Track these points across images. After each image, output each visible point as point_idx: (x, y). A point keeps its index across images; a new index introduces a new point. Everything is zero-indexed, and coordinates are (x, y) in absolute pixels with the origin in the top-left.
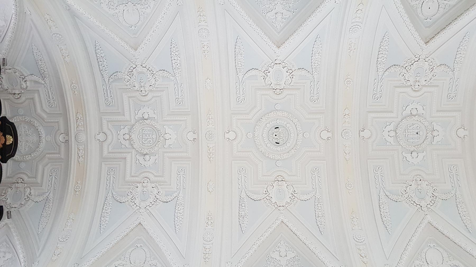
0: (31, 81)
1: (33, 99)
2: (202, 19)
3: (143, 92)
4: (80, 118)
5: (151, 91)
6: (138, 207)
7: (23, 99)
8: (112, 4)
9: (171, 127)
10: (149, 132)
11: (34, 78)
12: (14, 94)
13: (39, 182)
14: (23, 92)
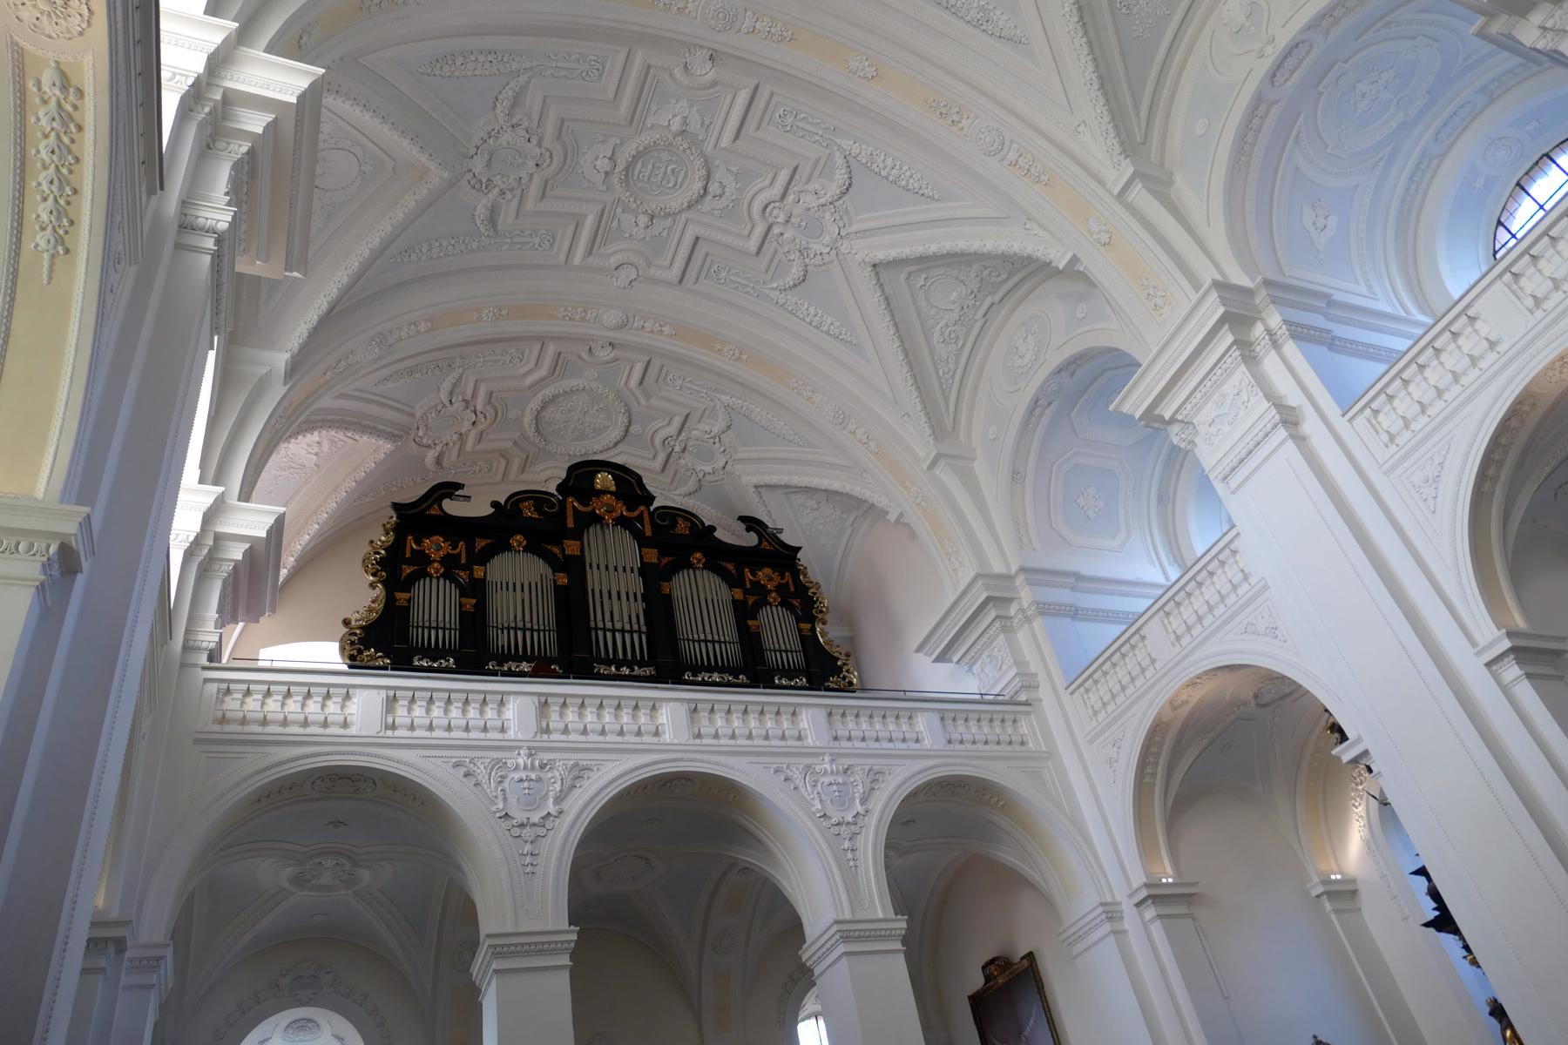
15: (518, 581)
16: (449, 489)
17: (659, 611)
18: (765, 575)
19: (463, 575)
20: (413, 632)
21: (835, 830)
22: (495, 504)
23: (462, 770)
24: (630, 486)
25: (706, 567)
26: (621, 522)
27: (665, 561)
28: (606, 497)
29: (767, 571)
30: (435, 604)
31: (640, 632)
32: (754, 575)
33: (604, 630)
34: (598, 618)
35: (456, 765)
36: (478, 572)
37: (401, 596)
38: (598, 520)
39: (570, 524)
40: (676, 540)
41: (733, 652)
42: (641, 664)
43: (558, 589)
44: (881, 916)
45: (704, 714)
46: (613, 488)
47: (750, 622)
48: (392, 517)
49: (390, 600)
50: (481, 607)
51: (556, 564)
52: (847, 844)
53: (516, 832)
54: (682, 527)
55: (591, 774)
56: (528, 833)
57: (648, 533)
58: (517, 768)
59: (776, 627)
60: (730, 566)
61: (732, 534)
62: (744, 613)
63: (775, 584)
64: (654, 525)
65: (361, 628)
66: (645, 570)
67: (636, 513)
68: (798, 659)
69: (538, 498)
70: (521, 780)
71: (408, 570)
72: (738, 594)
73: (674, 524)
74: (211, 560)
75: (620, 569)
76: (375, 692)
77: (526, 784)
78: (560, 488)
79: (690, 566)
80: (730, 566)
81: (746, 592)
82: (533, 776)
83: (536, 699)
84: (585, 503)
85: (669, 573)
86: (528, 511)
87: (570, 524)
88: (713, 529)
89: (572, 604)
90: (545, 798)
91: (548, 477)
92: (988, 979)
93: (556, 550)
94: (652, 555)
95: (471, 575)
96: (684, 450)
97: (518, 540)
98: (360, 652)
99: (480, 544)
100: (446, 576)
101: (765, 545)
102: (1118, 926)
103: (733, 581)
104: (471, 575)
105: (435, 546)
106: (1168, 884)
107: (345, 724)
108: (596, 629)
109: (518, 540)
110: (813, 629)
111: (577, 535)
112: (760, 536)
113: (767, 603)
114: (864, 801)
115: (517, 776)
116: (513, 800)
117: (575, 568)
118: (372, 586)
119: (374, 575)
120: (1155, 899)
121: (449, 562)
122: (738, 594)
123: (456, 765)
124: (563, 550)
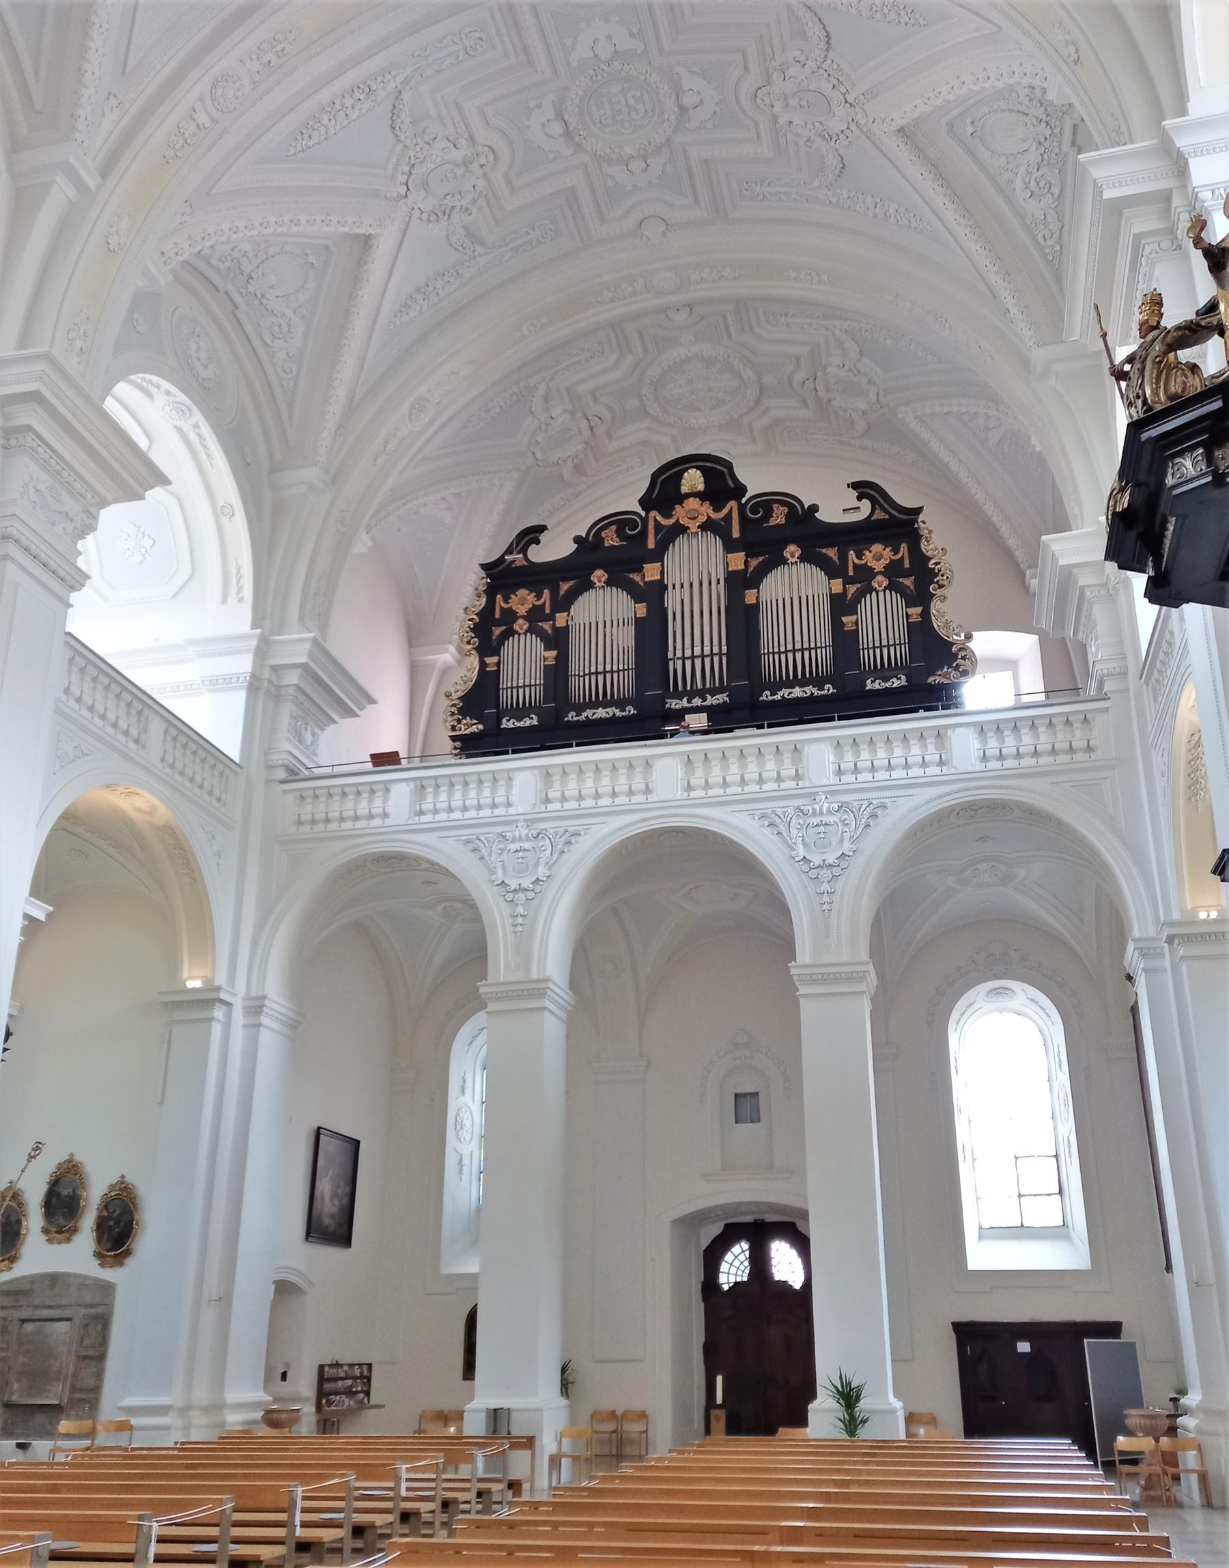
1: (593, 394)
2: (193, 127)
3: (483, 161)
4: (610, 295)
5: (472, 140)
6: (853, 126)
7: (598, 409)
8: (277, 329)
9: (569, 44)
10: (607, 106)
12: (592, 428)
13: (806, 349)
14: (580, 415)
16: (532, 535)
17: (743, 622)
18: (877, 556)
19: (547, 626)
21: (813, 874)
22: (577, 540)
23: (470, 847)
24: (721, 482)
25: (802, 559)
27: (754, 563)
28: (693, 503)
29: (877, 548)
30: (524, 661)
31: (720, 654)
32: (859, 556)
34: (677, 645)
35: (467, 842)
36: (561, 619)
37: (488, 660)
38: (680, 529)
39: (651, 544)
41: (824, 656)
42: (714, 692)
43: (639, 622)
44: (845, 959)
45: (698, 765)
46: (701, 487)
47: (844, 619)
49: (483, 665)
50: (563, 660)
51: (637, 593)
52: (825, 887)
53: (509, 897)
54: (779, 516)
55: (581, 839)
56: (521, 897)
57: (736, 534)
58: (514, 840)
60: (832, 553)
62: (840, 606)
63: (872, 564)
67: (725, 512)
68: (901, 652)
69: (621, 521)
70: (517, 851)
71: (497, 631)
73: (768, 514)
76: (404, 785)
77: (521, 854)
79: (784, 561)
80: (832, 553)
81: (848, 581)
82: (526, 845)
83: (536, 772)
84: (667, 515)
86: (611, 539)
87: (651, 544)
88: (814, 508)
89: (652, 633)
90: (537, 865)
91: (627, 497)
93: (636, 577)
94: (737, 561)
95: (554, 626)
96: (828, 390)
97: (599, 576)
98: (459, 721)
99: (565, 587)
100: (530, 630)
101: (879, 515)
103: (831, 570)
104: (554, 626)
105: (522, 601)
107: (385, 815)
109: (599, 576)
110: (926, 614)
111: (658, 555)
112: (874, 502)
113: (870, 590)
114: (854, 841)
115: (513, 847)
116: (510, 869)
117: (653, 595)
119: (469, 643)
121: (535, 615)
122: (837, 585)
124: (644, 576)
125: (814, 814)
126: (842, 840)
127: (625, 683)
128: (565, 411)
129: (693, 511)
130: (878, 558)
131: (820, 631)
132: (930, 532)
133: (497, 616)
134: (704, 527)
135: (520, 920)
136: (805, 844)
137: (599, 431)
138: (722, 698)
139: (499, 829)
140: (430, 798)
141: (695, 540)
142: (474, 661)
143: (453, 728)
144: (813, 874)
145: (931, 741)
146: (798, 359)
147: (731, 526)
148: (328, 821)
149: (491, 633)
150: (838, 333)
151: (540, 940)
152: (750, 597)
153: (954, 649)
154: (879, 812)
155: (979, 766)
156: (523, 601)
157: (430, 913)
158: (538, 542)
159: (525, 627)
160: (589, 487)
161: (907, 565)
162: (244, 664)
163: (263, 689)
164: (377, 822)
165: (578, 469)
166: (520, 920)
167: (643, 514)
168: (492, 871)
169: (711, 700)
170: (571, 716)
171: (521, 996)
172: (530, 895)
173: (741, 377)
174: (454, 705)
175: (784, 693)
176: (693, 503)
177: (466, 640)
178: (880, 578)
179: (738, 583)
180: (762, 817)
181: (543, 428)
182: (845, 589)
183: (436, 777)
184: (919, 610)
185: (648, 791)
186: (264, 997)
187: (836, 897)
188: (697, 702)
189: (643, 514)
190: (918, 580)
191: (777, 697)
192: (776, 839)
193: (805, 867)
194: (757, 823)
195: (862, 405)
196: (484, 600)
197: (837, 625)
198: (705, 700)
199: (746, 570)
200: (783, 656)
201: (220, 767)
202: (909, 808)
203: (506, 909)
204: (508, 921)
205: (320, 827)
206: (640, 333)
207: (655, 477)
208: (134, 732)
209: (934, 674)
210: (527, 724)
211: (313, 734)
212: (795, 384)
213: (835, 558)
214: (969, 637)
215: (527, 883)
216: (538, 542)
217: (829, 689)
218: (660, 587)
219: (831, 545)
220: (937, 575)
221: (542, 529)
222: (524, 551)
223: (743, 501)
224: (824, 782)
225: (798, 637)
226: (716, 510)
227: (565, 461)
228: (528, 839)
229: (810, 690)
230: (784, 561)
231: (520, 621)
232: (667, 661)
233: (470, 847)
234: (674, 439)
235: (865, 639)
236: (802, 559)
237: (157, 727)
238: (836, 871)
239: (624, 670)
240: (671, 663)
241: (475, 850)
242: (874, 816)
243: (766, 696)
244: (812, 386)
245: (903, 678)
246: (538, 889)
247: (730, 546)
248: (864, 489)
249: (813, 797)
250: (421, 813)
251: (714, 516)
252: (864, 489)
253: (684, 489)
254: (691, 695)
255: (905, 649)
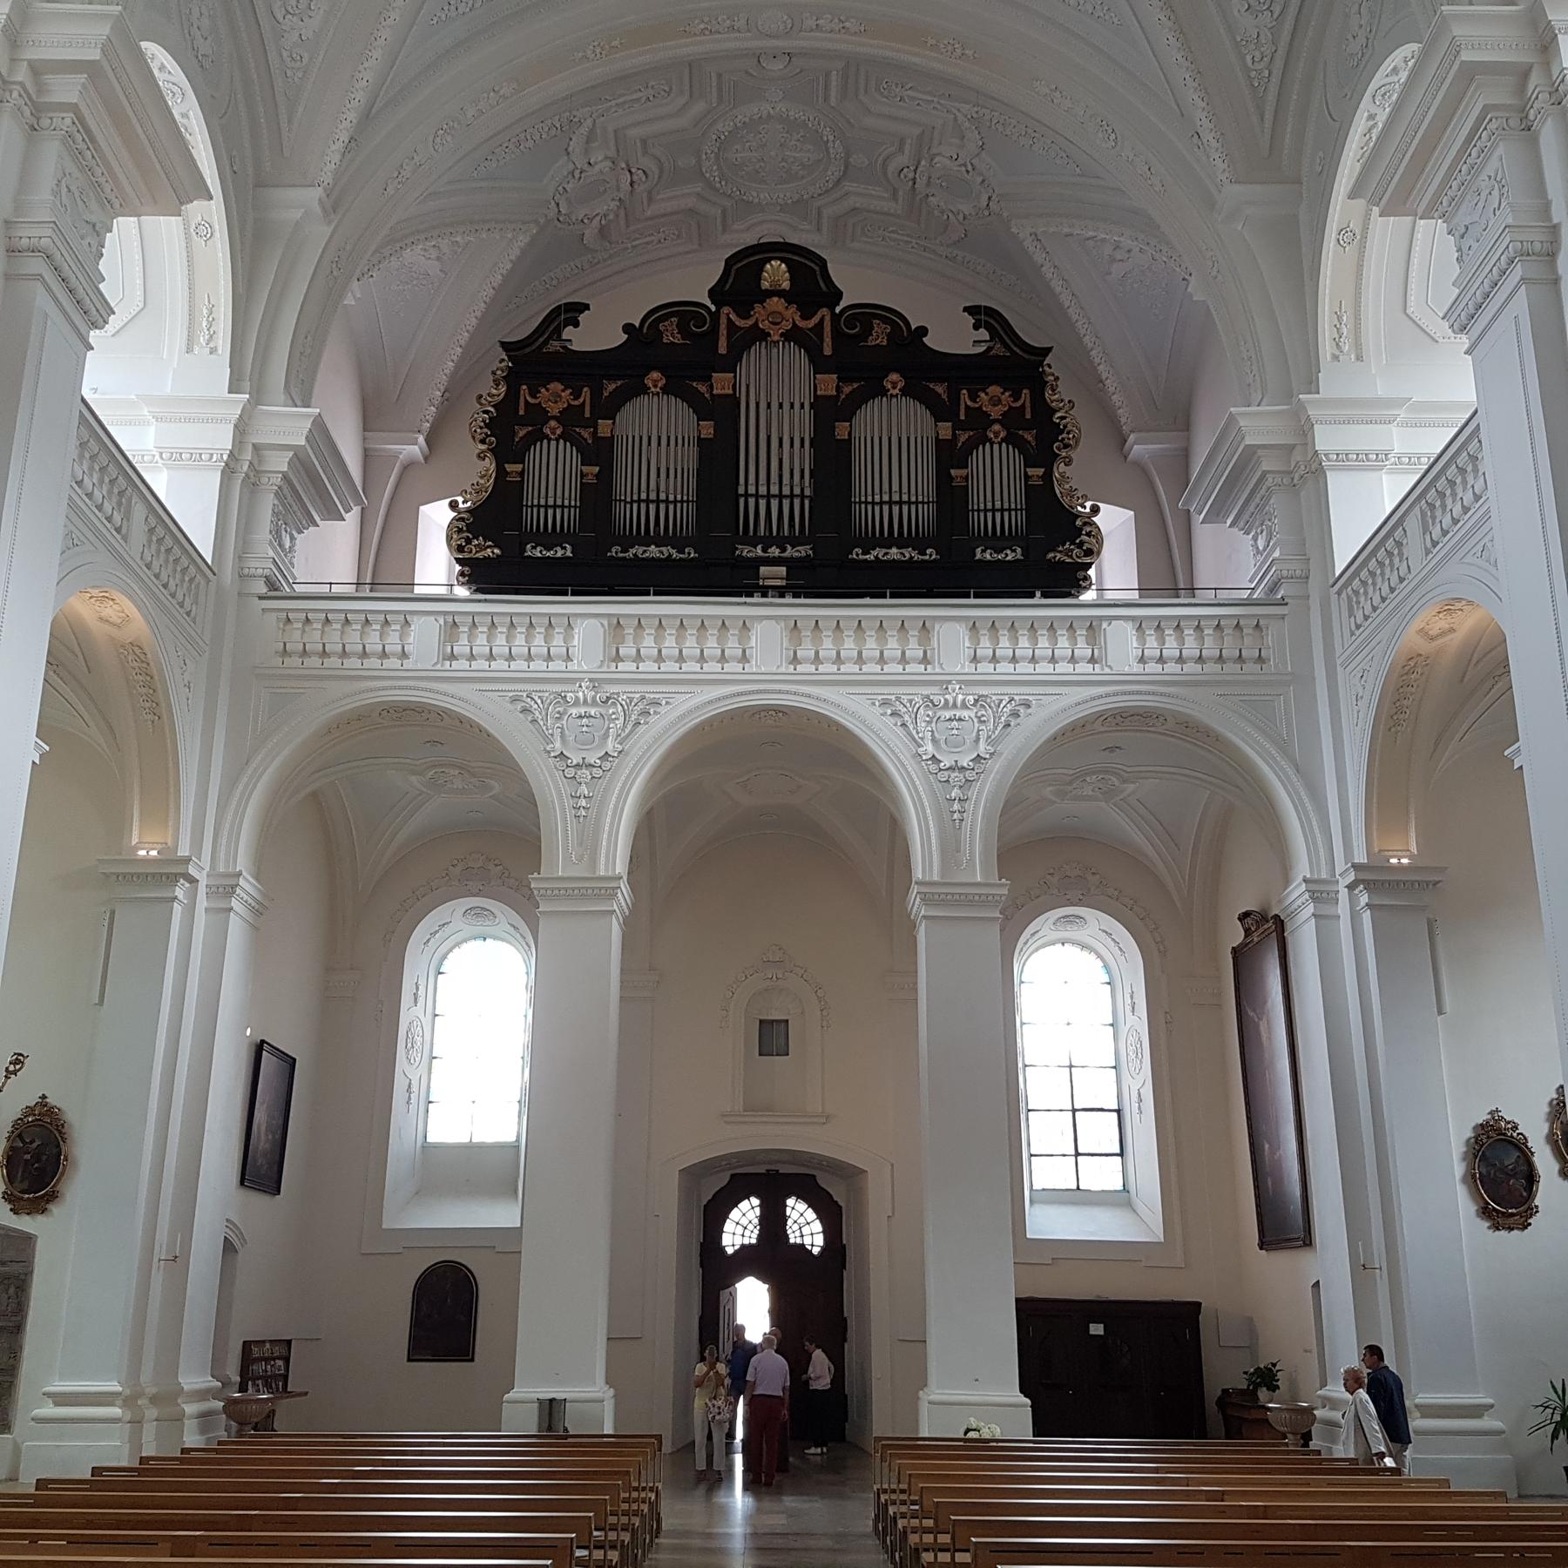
0: (587, 151)
1: (644, 142)
7: (647, 163)
11: (576, 145)
13: (917, 131)
15: (656, 437)
17: (832, 460)
18: (994, 400)
20: (527, 514)
21: (943, 776)
22: (628, 328)
23: (519, 706)
24: (811, 281)
25: (905, 392)
26: (792, 335)
27: (847, 390)
28: (776, 303)
29: (994, 390)
30: (555, 474)
31: (802, 496)
32: (973, 397)
33: (757, 496)
34: (750, 479)
35: (514, 700)
37: (509, 467)
39: (722, 350)
40: (870, 354)
41: (924, 515)
47: (953, 472)
48: (499, 360)
49: (500, 470)
51: (703, 408)
52: (955, 793)
53: (570, 772)
54: (879, 336)
57: (828, 351)
58: (576, 703)
59: (995, 477)
60: (940, 389)
61: (953, 336)
62: (949, 456)
64: (837, 334)
65: (469, 511)
66: (818, 403)
67: (815, 320)
68: (1017, 520)
69: (683, 312)
72: (945, 430)
73: (867, 330)
74: (256, 471)
75: (786, 406)
78: (712, 293)
79: (883, 392)
80: (940, 389)
81: (958, 426)
84: (748, 317)
85: (846, 409)
86: (671, 334)
87: (722, 350)
88: (923, 331)
89: (718, 460)
90: (606, 736)
91: (694, 282)
92: (1248, 932)
94: (828, 384)
96: (929, 184)
98: (468, 541)
101: (999, 350)
102: (1326, 910)
103: (940, 412)
105: (555, 397)
106: (1400, 868)
107: (404, 655)
108: (746, 495)
110: (1048, 476)
111: (730, 363)
112: (994, 334)
115: (574, 711)
117: (724, 413)
118: (481, 456)
119: (483, 442)
120: (1370, 886)
121: (570, 418)
122: (945, 430)
123: (514, 700)
124: (711, 387)
125: (946, 706)
126: (977, 740)
127: (683, 515)
128: (606, 158)
129: (776, 314)
130: (996, 402)
131: (923, 483)
132: (1057, 379)
133: (521, 412)
134: (788, 336)
135: (583, 803)
136: (934, 740)
137: (639, 189)
138: (803, 551)
139: (558, 688)
140: (464, 640)
141: (775, 350)
142: (490, 464)
143: (460, 549)
144: (943, 776)
145: (1081, 632)
146: (902, 142)
147: (822, 341)
148: (324, 654)
149: (514, 433)
150: (960, 117)
151: (598, 830)
152: (841, 430)
153: (1078, 523)
154: (1022, 710)
155: (1138, 668)
156: (557, 397)
157: (413, 778)
158: (576, 325)
159: (558, 432)
160: (611, 257)
161: (1028, 416)
162: (223, 439)
163: (240, 473)
164: (393, 663)
165: (603, 232)
166: (583, 803)
167: (713, 308)
168: (548, 739)
169: (789, 552)
170: (615, 551)
171: (583, 896)
172: (597, 772)
173: (827, 150)
174: (462, 519)
175: (878, 553)
176: (776, 303)
177: (478, 437)
178: (997, 427)
179: (828, 413)
180: (885, 703)
181: (577, 174)
182: (954, 434)
183: (473, 614)
184: (1041, 471)
185: (744, 659)
186: (240, 874)
187: (969, 806)
188: (774, 551)
189: (713, 308)
190: (1042, 438)
191: (870, 557)
192: (900, 731)
193: (933, 768)
194: (878, 710)
195: (966, 208)
196: (503, 389)
197: (943, 478)
198: (784, 550)
199: (838, 396)
200: (877, 508)
201: (192, 569)
202: (1053, 710)
203: (566, 789)
204: (569, 803)
205: (314, 661)
206: (720, 76)
207: (729, 262)
208: (117, 518)
209: (1054, 550)
210: (559, 555)
211: (292, 538)
212: (892, 167)
213: (944, 397)
214: (1095, 510)
215: (593, 758)
216: (576, 325)
217: (931, 554)
218: (733, 401)
219: (941, 380)
220: (1062, 432)
221: (587, 307)
222: (558, 332)
223: (838, 310)
224: (957, 670)
225: (895, 487)
226: (804, 317)
227: (591, 220)
228: (594, 703)
229: (908, 553)
230: (883, 392)
231: (553, 423)
232: (738, 496)
233: (519, 706)
234: (724, 212)
235: (977, 499)
236: (904, 392)
237: (139, 511)
238: (970, 775)
239: (682, 501)
240: (742, 501)
241: (524, 710)
242: (1015, 714)
243: (856, 554)
244: (911, 175)
245: (1019, 550)
246: (607, 765)
247: (819, 364)
248: (983, 316)
249: (944, 685)
250: (453, 657)
251: (801, 324)
252: (983, 316)
253: (765, 285)
254: (767, 542)
255: (1021, 518)
